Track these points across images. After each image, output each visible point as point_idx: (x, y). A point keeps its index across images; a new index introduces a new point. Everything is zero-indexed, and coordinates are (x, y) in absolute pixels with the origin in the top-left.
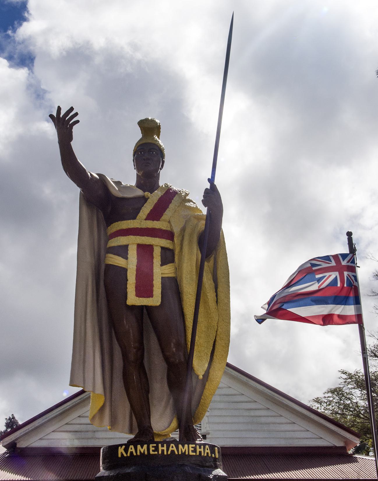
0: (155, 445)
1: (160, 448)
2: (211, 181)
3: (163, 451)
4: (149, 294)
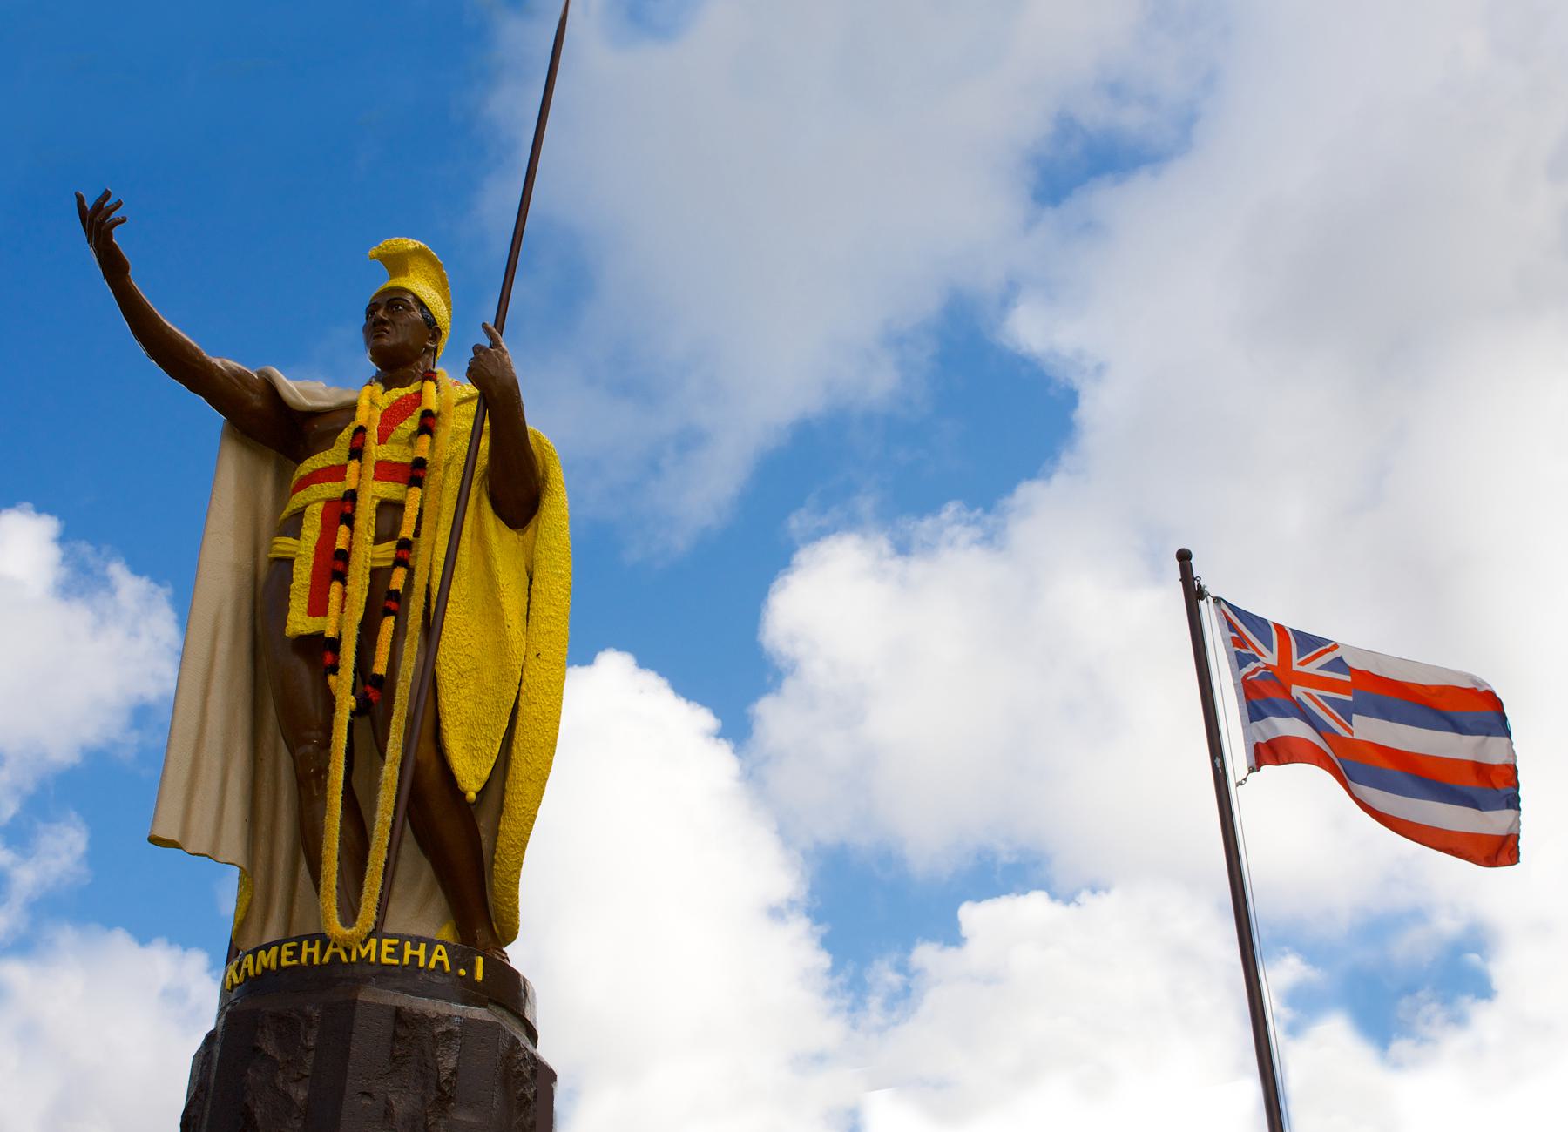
3: (311, 956)
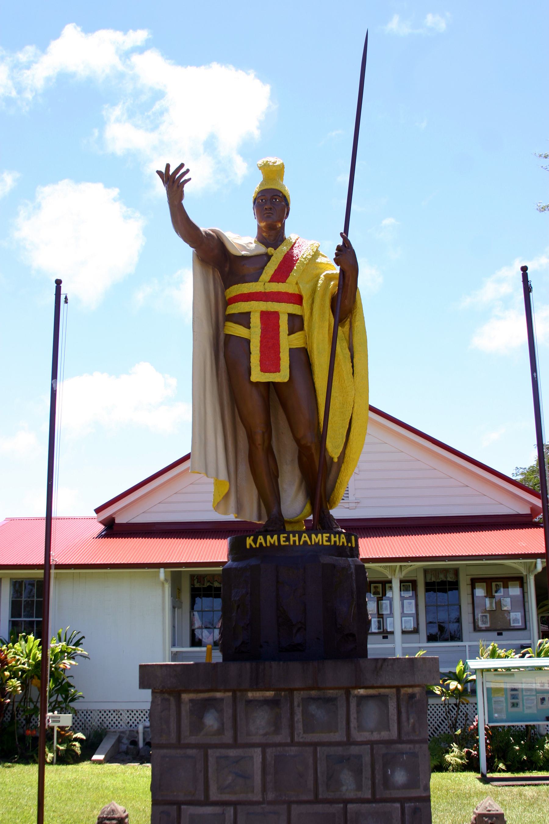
0: (286, 535)
1: (292, 539)
4: (277, 369)
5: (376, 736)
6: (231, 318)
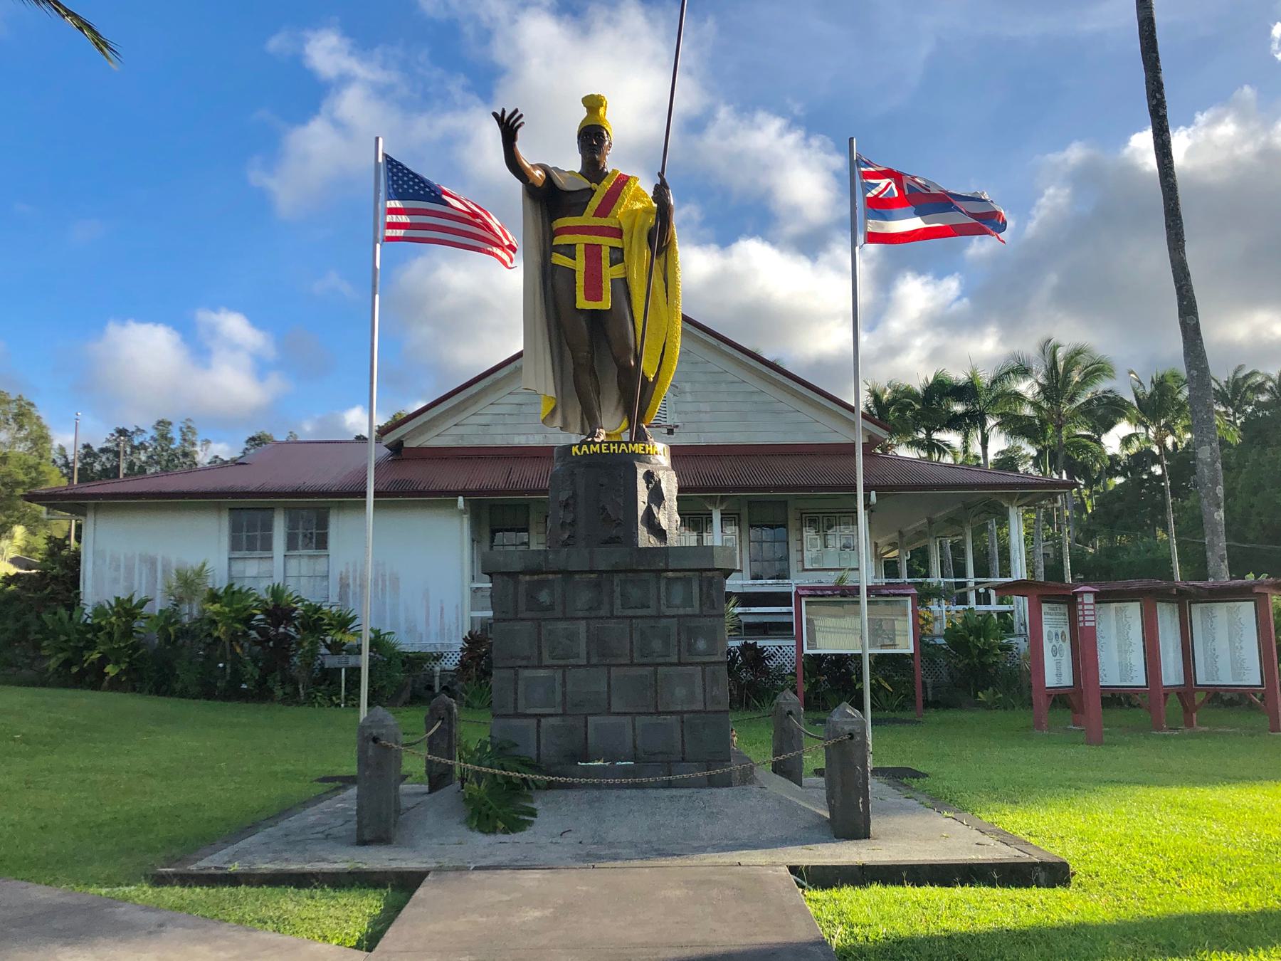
2: (661, 175)
4: (598, 298)
5: (681, 611)
6: (557, 249)
